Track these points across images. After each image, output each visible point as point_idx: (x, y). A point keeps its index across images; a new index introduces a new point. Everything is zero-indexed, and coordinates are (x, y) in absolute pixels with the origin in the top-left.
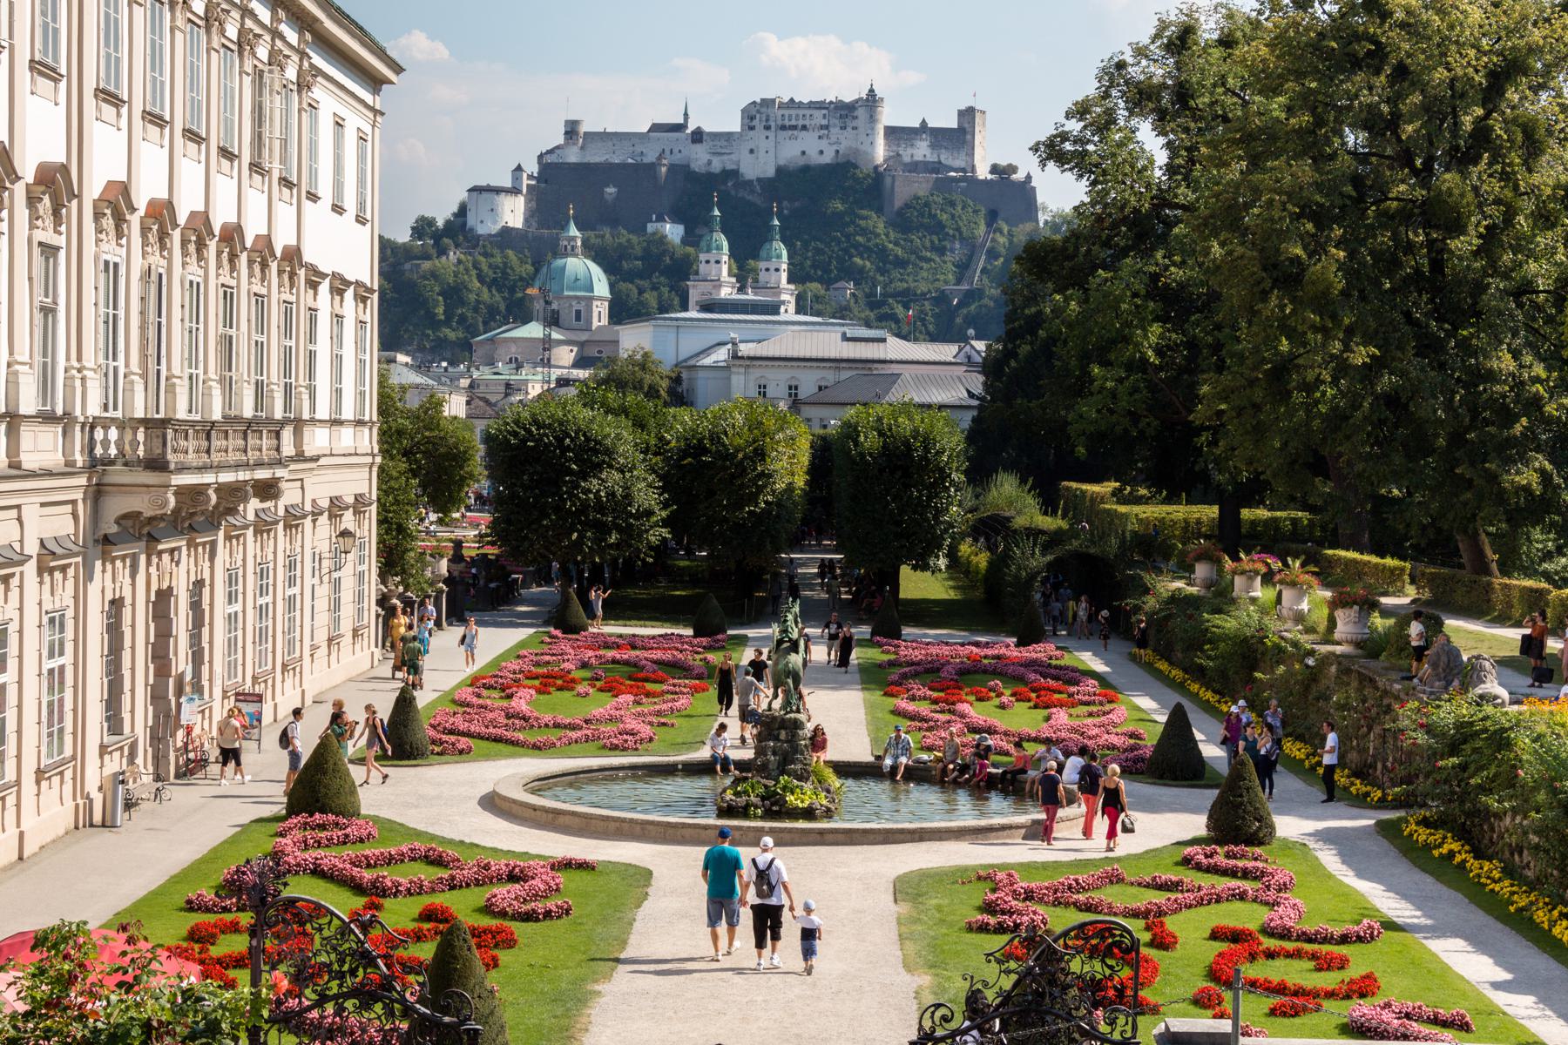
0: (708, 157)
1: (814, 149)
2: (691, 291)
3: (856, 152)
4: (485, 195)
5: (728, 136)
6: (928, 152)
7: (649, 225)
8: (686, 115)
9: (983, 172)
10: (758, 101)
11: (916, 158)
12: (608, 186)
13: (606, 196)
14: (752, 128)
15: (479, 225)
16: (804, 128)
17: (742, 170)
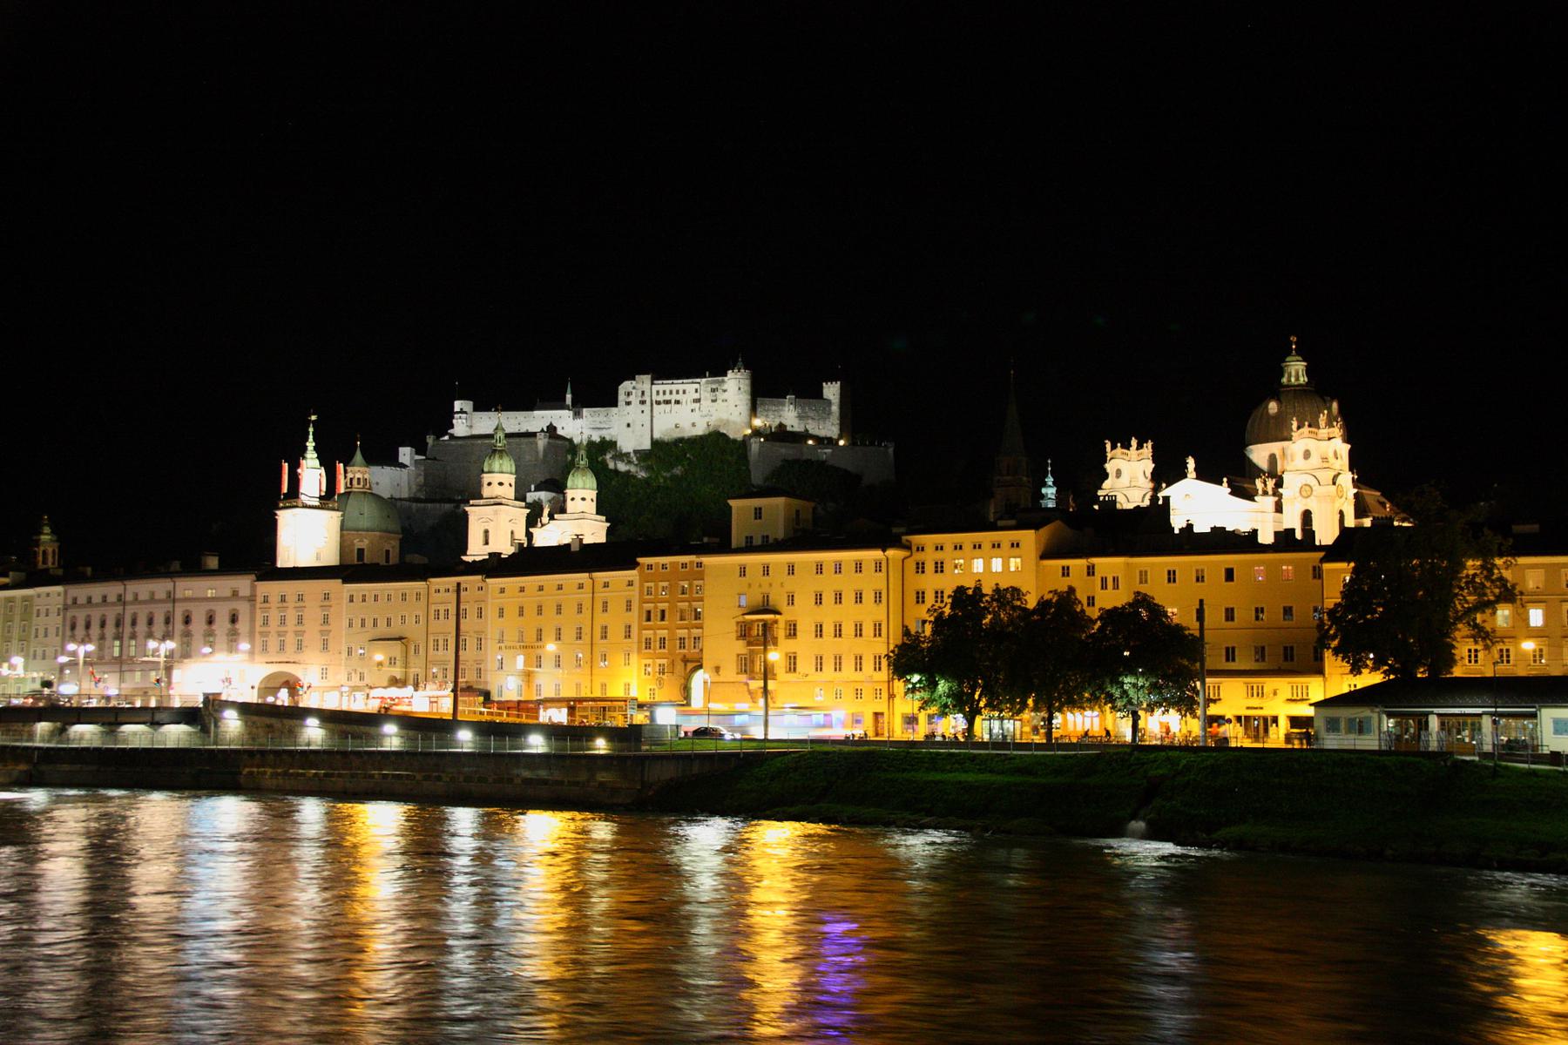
7: (528, 495)
14: (628, 403)
16: (677, 402)
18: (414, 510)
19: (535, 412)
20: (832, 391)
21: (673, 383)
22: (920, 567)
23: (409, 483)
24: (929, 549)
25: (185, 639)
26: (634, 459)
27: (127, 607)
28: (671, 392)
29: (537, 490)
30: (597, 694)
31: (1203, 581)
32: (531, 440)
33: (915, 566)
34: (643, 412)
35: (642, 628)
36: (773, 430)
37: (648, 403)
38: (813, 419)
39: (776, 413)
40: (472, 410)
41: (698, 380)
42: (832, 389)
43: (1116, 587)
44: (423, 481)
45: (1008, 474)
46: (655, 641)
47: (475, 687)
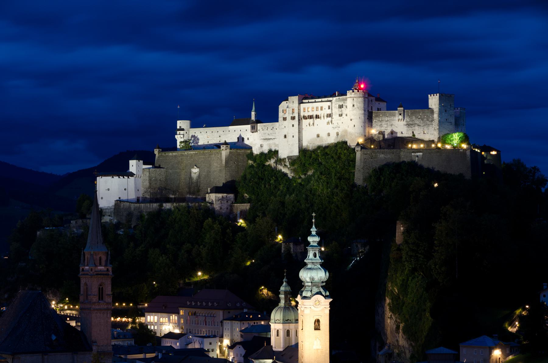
0: (261, 142)
11: (394, 135)
12: (193, 168)
13: (193, 175)
14: (285, 119)
16: (317, 117)
18: (133, 209)
19: (230, 127)
20: (434, 101)
21: (315, 102)
23: (136, 187)
26: (288, 164)
29: (212, 192)
32: (218, 150)
34: (293, 126)
36: (386, 137)
38: (419, 125)
39: (388, 123)
40: (189, 126)
41: (331, 99)
42: (434, 100)
44: (148, 184)
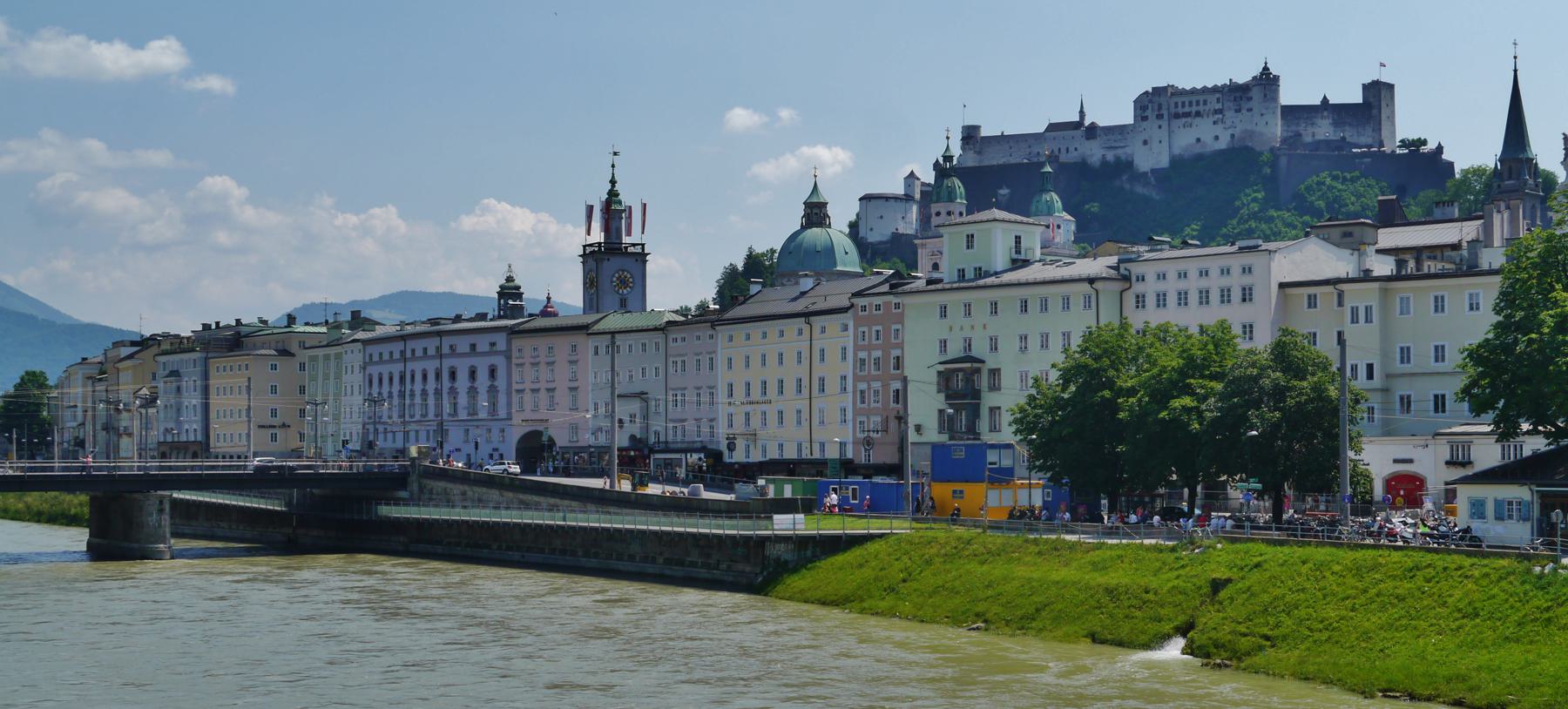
0: (1103, 152)
1: (1209, 135)
2: (919, 251)
3: (1250, 134)
4: (873, 202)
5: (1120, 130)
6: (1331, 129)
8: (1082, 113)
9: (1392, 146)
10: (1150, 90)
11: (1318, 137)
12: (1001, 188)
14: (1145, 118)
15: (869, 232)
16: (1198, 114)
17: (1135, 162)
22: (1140, 301)
24: (1151, 278)
25: (424, 397)
26: (1152, 179)
27: (408, 364)
28: (1190, 104)
30: (817, 455)
31: (1478, 309)
33: (1134, 300)
34: (1160, 127)
35: (856, 379)
37: (1166, 117)
38: (1350, 125)
43: (1368, 320)
45: (1510, 178)
46: (869, 395)
47: (710, 447)
